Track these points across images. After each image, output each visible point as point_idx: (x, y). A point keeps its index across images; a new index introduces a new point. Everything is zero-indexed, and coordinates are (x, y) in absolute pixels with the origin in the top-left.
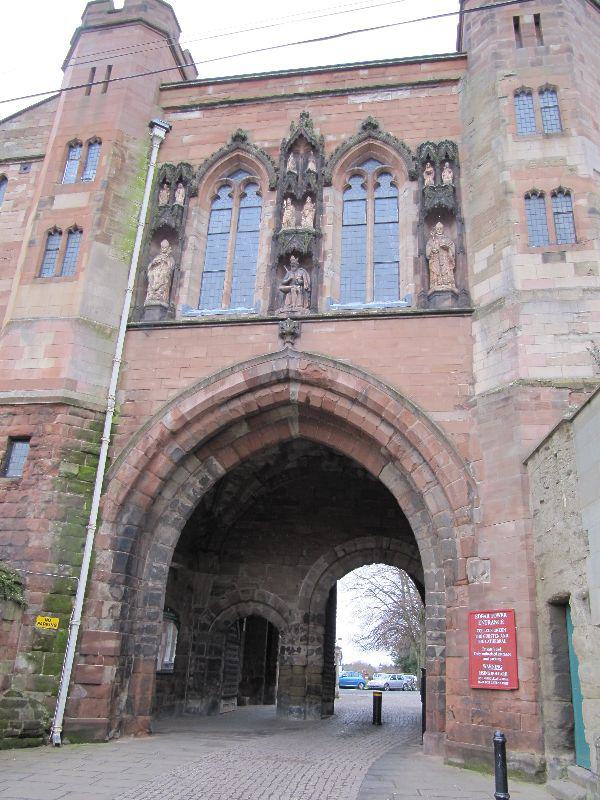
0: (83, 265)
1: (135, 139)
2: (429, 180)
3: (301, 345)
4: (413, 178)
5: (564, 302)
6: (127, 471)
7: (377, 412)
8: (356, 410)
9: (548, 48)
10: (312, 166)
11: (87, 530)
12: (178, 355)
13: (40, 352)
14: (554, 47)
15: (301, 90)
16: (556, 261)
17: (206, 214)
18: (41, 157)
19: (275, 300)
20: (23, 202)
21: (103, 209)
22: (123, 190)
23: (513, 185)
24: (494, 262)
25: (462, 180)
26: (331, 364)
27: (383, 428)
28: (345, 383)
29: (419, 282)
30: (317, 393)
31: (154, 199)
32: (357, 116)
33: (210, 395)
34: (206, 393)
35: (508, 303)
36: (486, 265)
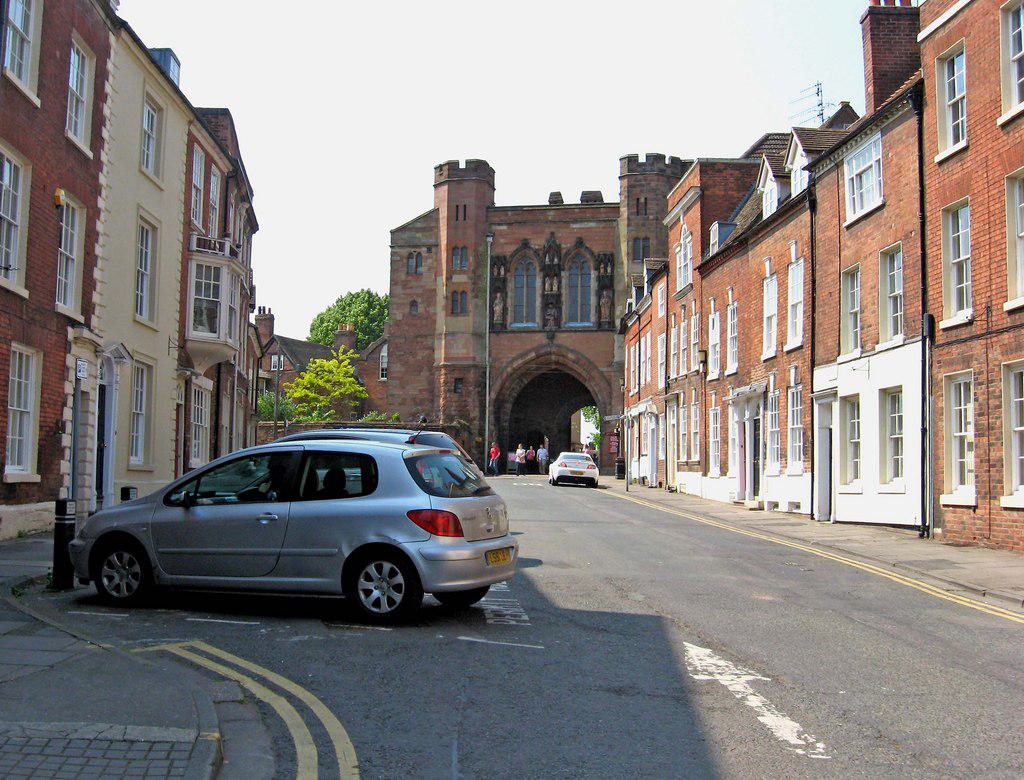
2: (602, 271)
3: (555, 342)
4: (597, 269)
13: (460, 346)
14: (651, 217)
19: (545, 323)
21: (474, 283)
31: (492, 273)
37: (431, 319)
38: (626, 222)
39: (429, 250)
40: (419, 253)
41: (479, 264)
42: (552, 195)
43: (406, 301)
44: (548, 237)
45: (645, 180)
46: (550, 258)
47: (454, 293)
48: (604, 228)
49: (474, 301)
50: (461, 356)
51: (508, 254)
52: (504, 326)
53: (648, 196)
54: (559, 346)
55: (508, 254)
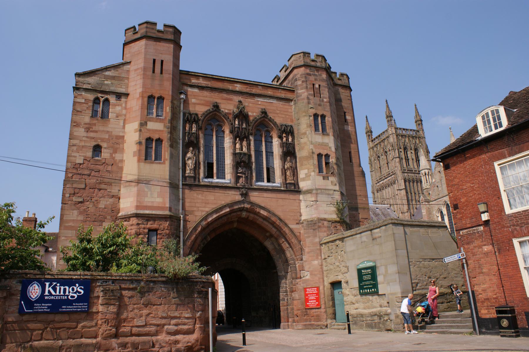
2: (284, 139)
4: (280, 137)
5: (329, 194)
8: (265, 222)
9: (323, 100)
10: (244, 126)
12: (203, 198)
13: (156, 195)
15: (237, 89)
16: (326, 179)
19: (237, 178)
20: (121, 115)
21: (171, 133)
23: (314, 151)
24: (308, 176)
25: (295, 141)
27: (273, 229)
30: (252, 215)
31: (184, 128)
32: (259, 106)
35: (314, 192)
36: (305, 176)
38: (306, 101)
40: (107, 101)
43: (88, 144)
46: (239, 122)
47: (149, 140)
50: (155, 205)
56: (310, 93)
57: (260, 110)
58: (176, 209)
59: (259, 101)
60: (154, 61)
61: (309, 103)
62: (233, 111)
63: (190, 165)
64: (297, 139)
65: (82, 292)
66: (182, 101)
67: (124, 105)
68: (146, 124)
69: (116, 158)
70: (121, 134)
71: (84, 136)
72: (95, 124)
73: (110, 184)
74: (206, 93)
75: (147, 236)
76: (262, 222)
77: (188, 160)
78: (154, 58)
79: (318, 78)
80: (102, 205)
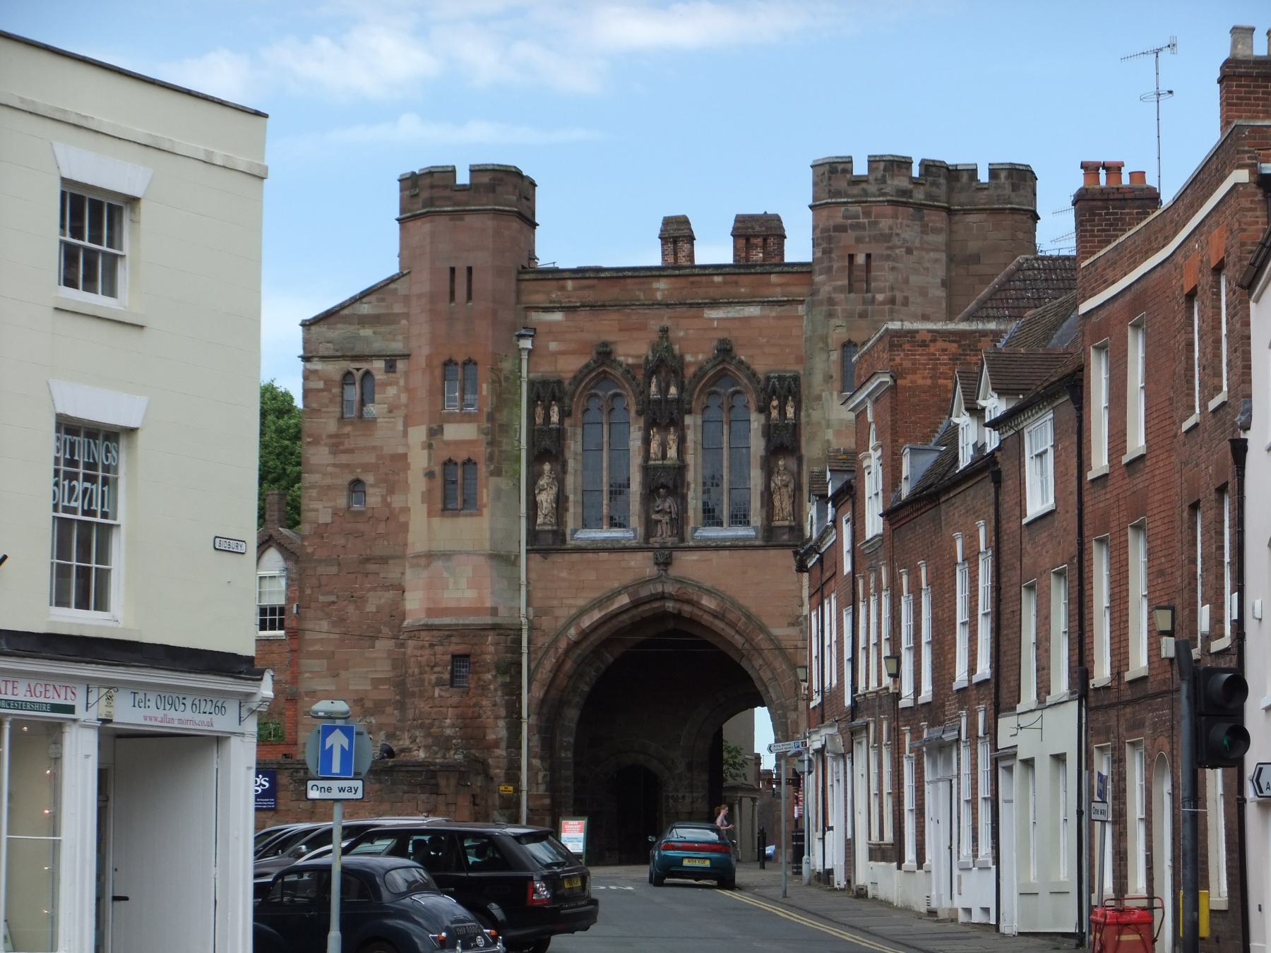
0: (485, 500)
1: (506, 356)
2: (775, 414)
3: (673, 572)
4: (763, 409)
6: (544, 673)
7: (732, 625)
8: (717, 622)
9: (874, 297)
11: (521, 722)
13: (463, 583)
14: (880, 297)
15: (659, 296)
17: (579, 430)
18: (406, 356)
19: (650, 527)
21: (491, 443)
22: (503, 417)
25: (803, 414)
26: (697, 589)
27: (737, 637)
28: (707, 604)
29: (764, 516)
33: (603, 613)
34: (600, 611)
37: (395, 522)
39: (391, 367)
40: (368, 373)
41: (504, 398)
42: (668, 222)
43: (339, 482)
44: (655, 337)
45: (867, 214)
46: (659, 386)
48: (778, 318)
49: (494, 481)
51: (567, 376)
52: (559, 535)
53: (876, 250)
54: (677, 580)
55: (567, 376)
56: (839, 283)
57: (715, 343)
58: (511, 608)
59: (713, 319)
60: (453, 270)
61: (831, 315)
62: (647, 357)
63: (545, 504)
64: (807, 410)
65: (267, 785)
66: (525, 356)
67: (402, 382)
68: (441, 430)
69: (393, 506)
70: (401, 450)
71: (328, 465)
72: (348, 435)
73: (384, 560)
74: (582, 317)
75: (449, 668)
76: (712, 622)
77: (539, 493)
78: (453, 266)
79: (866, 233)
80: (371, 608)
